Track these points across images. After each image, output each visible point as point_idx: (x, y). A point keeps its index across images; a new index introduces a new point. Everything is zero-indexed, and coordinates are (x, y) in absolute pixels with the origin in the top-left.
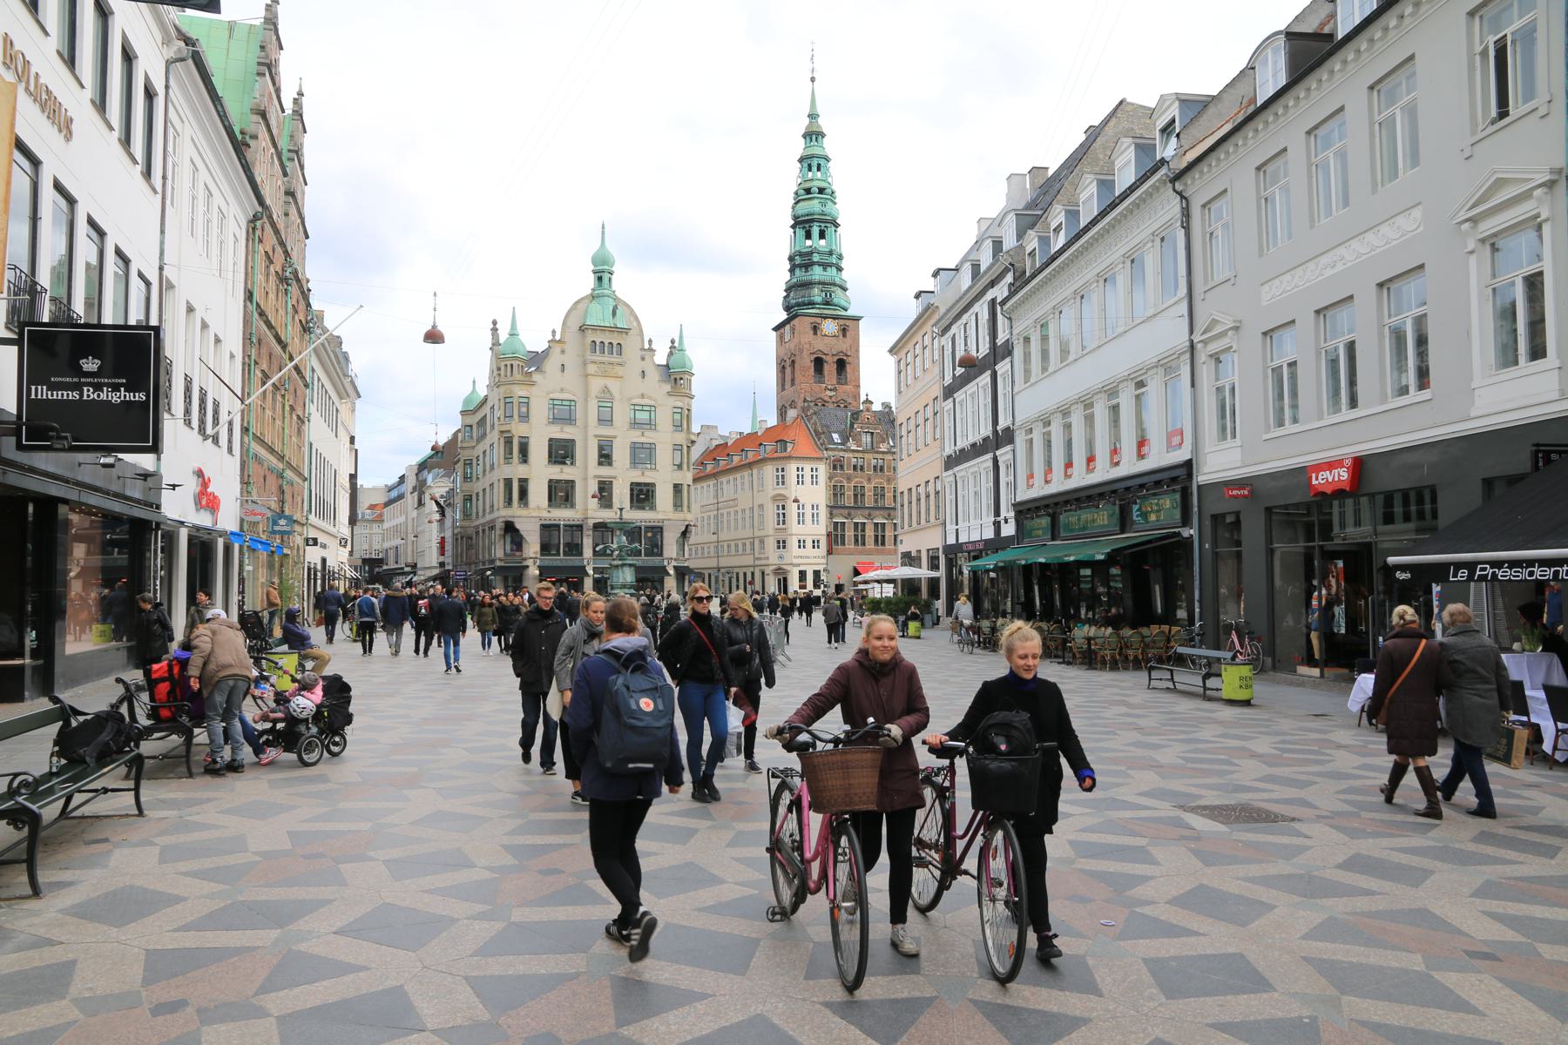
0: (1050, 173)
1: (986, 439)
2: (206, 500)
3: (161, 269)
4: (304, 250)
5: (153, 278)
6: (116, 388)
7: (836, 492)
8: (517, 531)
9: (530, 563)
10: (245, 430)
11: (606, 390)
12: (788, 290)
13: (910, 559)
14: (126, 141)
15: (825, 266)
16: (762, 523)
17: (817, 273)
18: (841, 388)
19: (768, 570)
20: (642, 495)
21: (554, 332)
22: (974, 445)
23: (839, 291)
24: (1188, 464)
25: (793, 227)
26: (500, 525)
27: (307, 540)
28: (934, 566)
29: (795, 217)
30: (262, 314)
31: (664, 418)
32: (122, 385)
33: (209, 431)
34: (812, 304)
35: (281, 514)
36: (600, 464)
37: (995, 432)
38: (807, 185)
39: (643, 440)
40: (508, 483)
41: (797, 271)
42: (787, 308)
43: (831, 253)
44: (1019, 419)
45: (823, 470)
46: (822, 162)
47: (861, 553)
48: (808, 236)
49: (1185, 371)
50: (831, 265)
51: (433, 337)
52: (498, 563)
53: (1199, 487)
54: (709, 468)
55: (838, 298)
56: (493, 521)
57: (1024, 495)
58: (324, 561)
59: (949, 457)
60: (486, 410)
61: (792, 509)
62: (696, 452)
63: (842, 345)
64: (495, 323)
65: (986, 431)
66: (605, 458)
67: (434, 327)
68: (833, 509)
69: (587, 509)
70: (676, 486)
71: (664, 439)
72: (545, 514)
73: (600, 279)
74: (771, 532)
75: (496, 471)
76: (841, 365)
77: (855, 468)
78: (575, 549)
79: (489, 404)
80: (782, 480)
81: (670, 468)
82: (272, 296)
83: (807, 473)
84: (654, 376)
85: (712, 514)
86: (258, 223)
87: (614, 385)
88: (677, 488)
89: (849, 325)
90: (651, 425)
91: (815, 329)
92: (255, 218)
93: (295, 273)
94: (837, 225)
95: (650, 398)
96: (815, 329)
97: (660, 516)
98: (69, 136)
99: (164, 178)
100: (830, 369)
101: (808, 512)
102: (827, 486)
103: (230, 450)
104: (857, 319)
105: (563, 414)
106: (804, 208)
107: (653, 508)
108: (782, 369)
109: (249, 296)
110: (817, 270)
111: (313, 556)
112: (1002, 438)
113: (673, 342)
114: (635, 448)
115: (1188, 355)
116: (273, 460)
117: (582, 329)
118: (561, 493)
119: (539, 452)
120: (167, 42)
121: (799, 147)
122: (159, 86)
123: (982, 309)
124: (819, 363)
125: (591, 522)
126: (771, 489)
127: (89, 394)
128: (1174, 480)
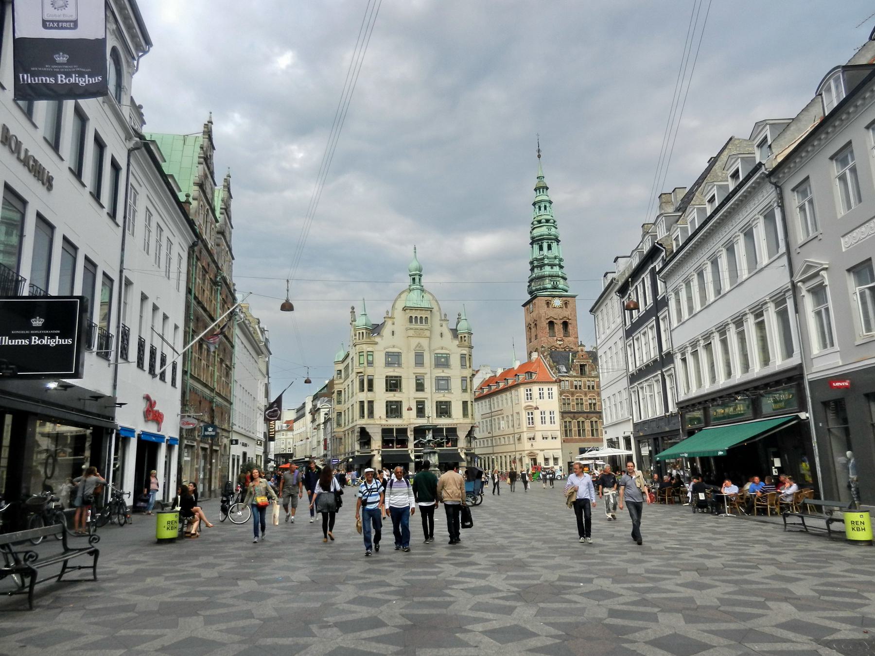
0: (687, 190)
1: (655, 361)
2: (152, 414)
3: (121, 272)
4: (231, 266)
5: (115, 277)
6: (53, 336)
7: (564, 403)
8: (368, 433)
9: (375, 452)
10: (185, 373)
11: (419, 345)
12: (531, 281)
13: (612, 443)
14: (96, 195)
15: (552, 266)
16: (519, 425)
17: (547, 270)
18: (567, 339)
20: (443, 409)
21: (388, 312)
22: (647, 366)
23: (562, 281)
24: (800, 367)
25: (532, 244)
26: (357, 430)
27: (231, 441)
28: (628, 447)
29: (533, 238)
30: (199, 303)
31: (455, 361)
32: (57, 334)
33: (158, 370)
35: (212, 425)
36: (417, 390)
37: (661, 356)
38: (539, 218)
39: (443, 375)
40: (362, 403)
41: (536, 270)
42: (531, 293)
43: (555, 258)
44: (676, 346)
45: (555, 389)
46: (548, 205)
48: (541, 249)
49: (790, 304)
50: (555, 265)
51: (287, 307)
52: (357, 454)
53: (810, 383)
54: (486, 391)
55: (561, 284)
56: (353, 427)
57: (682, 397)
58: (245, 454)
59: (632, 375)
60: (349, 360)
61: (537, 415)
62: (477, 382)
63: (566, 313)
64: (353, 308)
65: (654, 354)
66: (420, 387)
67: (287, 301)
68: (563, 414)
69: (409, 419)
71: (455, 372)
72: (384, 422)
73: (414, 279)
74: (525, 429)
75: (355, 397)
76: (565, 324)
77: (576, 387)
78: (403, 443)
79: (350, 357)
80: (530, 397)
81: (460, 391)
82: (207, 293)
83: (546, 392)
84: (448, 335)
85: (488, 420)
86: (196, 248)
87: (424, 342)
88: (465, 403)
89: (568, 300)
91: (548, 304)
92: (194, 244)
93: (224, 279)
94: (558, 241)
95: (446, 349)
96: (548, 304)
97: (455, 422)
98: (50, 188)
99: (125, 217)
100: (559, 328)
102: (560, 400)
103: (173, 384)
105: (393, 359)
106: (537, 232)
107: (450, 416)
108: (529, 328)
109: (189, 291)
110: (547, 268)
111: (236, 450)
112: (665, 360)
115: (791, 292)
116: (207, 391)
117: (405, 309)
118: (394, 409)
119: (380, 385)
120: (128, 138)
122: (123, 163)
123: (646, 276)
124: (551, 324)
125: (413, 426)
126: (524, 403)
127: (35, 341)
128: (790, 379)
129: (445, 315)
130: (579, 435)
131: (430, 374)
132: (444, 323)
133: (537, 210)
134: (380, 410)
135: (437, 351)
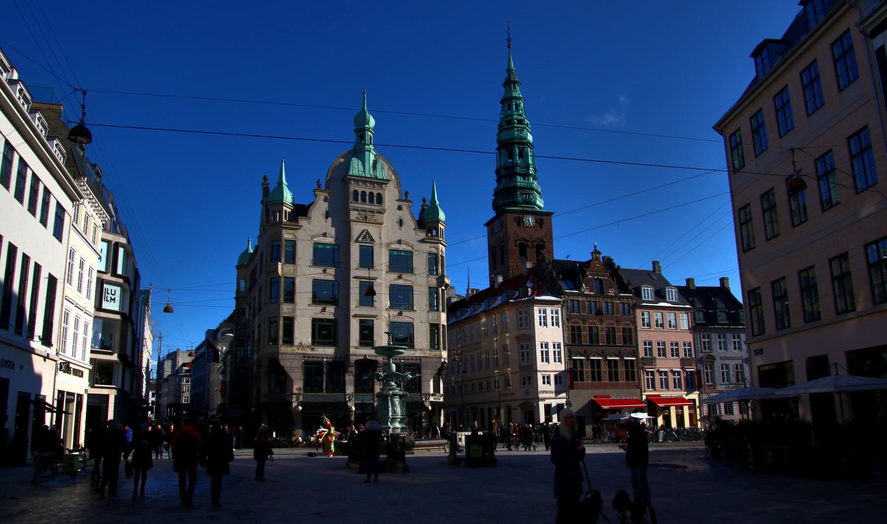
8: (282, 367)
11: (367, 235)
12: (497, 194)
19: (514, 405)
20: (402, 335)
25: (498, 149)
31: (420, 263)
34: (516, 204)
38: (509, 119)
41: (503, 181)
42: (495, 207)
47: (598, 387)
48: (511, 155)
52: (263, 399)
63: (540, 234)
70: (432, 325)
71: (420, 281)
72: (309, 351)
87: (373, 230)
90: (410, 270)
95: (407, 244)
96: (520, 222)
97: (418, 354)
100: (530, 252)
101: (551, 350)
104: (549, 214)
106: (505, 136)
113: (424, 200)
114: (393, 289)
121: (501, 93)
129: (406, 193)
130: (593, 379)
131: (384, 280)
132: (405, 206)
133: (506, 108)
134: (303, 333)
135: (394, 246)
